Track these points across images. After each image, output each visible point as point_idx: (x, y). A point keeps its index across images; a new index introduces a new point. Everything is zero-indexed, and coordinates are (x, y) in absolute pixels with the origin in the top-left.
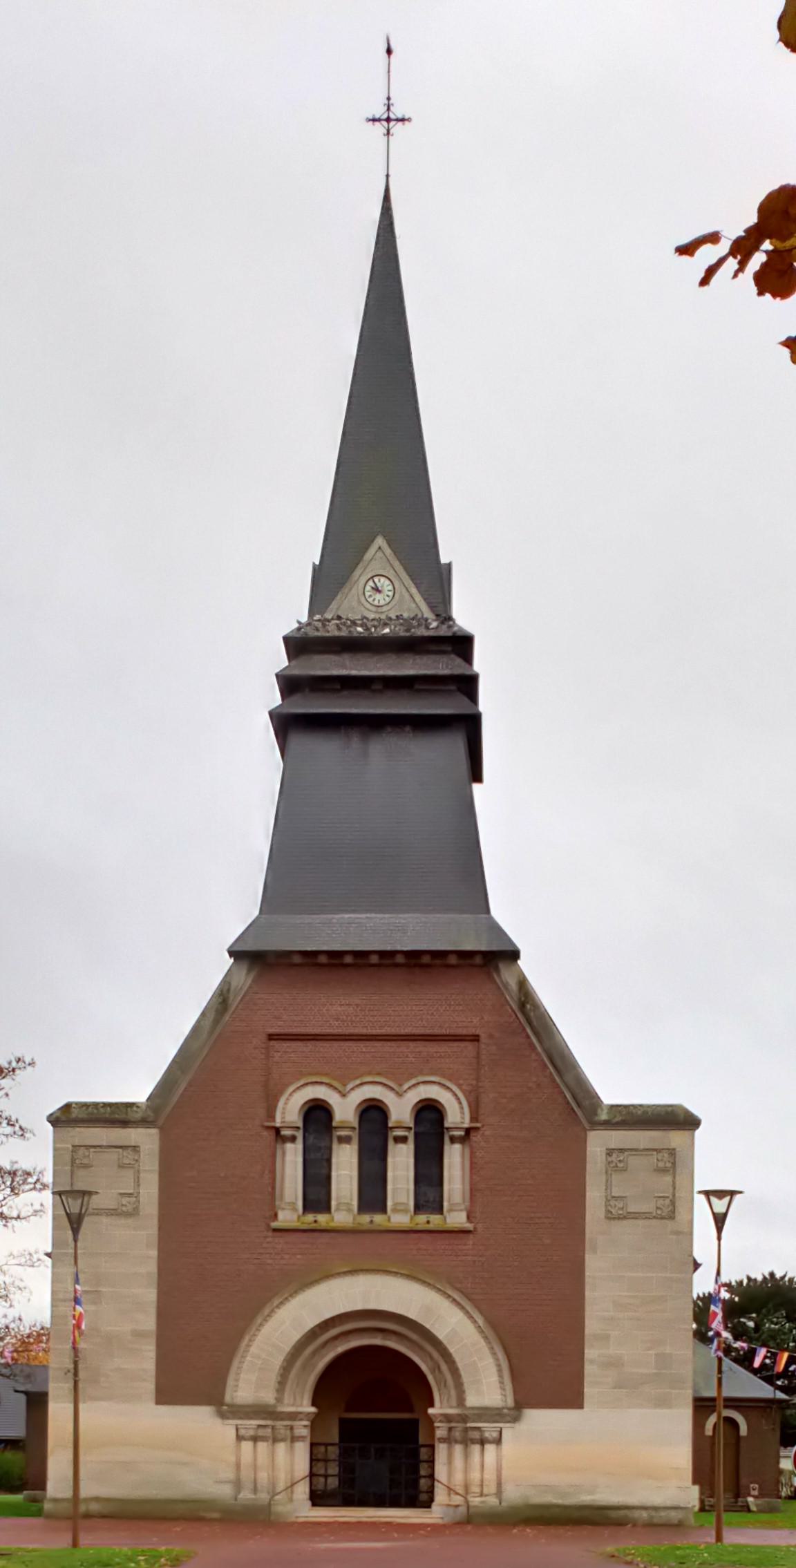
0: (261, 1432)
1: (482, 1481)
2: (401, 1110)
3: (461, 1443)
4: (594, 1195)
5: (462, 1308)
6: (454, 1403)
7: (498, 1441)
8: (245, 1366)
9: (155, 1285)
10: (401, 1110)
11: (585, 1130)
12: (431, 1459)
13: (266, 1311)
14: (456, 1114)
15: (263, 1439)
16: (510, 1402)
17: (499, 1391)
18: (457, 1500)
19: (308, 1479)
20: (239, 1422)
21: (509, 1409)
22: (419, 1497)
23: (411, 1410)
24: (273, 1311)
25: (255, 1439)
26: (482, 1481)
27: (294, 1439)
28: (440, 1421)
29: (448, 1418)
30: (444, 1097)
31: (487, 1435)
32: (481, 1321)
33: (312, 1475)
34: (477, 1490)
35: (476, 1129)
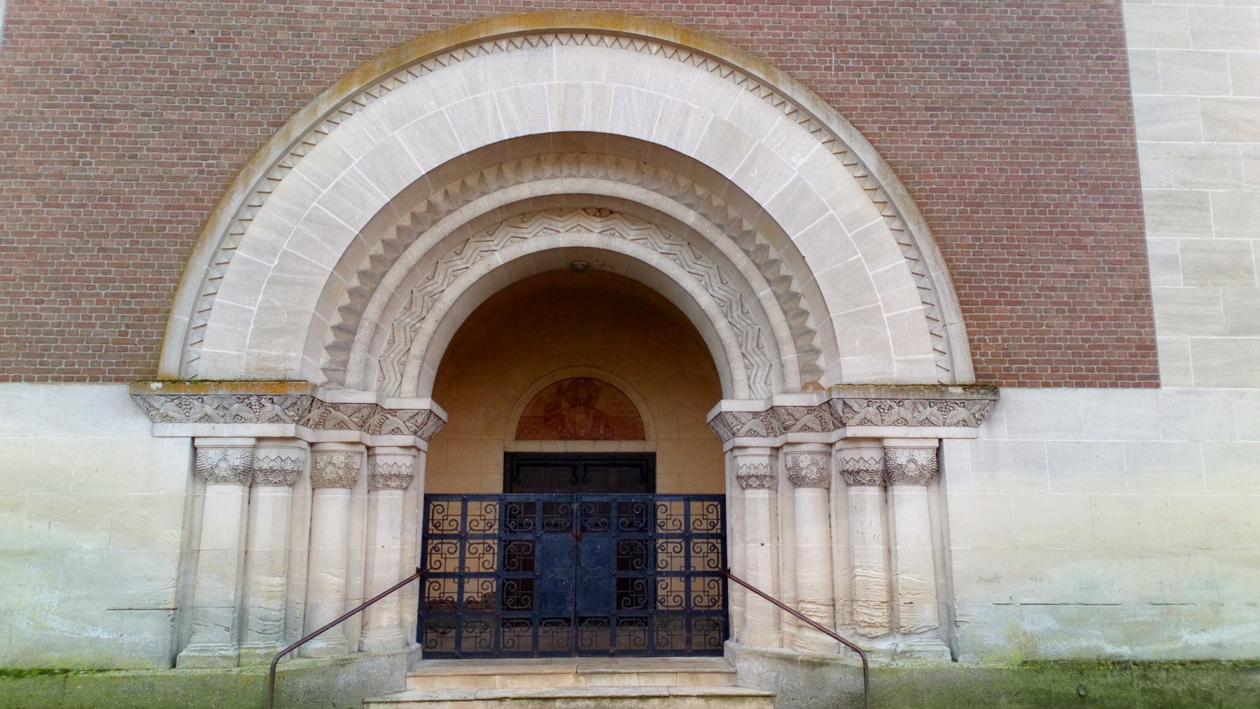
0: (268, 457)
1: (891, 589)
3: (814, 484)
5: (820, 128)
6: (794, 381)
7: (936, 473)
8: (230, 273)
12: (717, 530)
13: (298, 126)
15: (286, 478)
16: (965, 373)
17: (928, 342)
18: (814, 644)
19: (417, 582)
20: (202, 429)
21: (965, 387)
23: (638, 434)
24: (314, 129)
25: (249, 476)
26: (891, 589)
27: (377, 481)
28: (752, 433)
29: (775, 420)
31: (901, 458)
32: (870, 159)
33: (424, 574)
34: (880, 616)
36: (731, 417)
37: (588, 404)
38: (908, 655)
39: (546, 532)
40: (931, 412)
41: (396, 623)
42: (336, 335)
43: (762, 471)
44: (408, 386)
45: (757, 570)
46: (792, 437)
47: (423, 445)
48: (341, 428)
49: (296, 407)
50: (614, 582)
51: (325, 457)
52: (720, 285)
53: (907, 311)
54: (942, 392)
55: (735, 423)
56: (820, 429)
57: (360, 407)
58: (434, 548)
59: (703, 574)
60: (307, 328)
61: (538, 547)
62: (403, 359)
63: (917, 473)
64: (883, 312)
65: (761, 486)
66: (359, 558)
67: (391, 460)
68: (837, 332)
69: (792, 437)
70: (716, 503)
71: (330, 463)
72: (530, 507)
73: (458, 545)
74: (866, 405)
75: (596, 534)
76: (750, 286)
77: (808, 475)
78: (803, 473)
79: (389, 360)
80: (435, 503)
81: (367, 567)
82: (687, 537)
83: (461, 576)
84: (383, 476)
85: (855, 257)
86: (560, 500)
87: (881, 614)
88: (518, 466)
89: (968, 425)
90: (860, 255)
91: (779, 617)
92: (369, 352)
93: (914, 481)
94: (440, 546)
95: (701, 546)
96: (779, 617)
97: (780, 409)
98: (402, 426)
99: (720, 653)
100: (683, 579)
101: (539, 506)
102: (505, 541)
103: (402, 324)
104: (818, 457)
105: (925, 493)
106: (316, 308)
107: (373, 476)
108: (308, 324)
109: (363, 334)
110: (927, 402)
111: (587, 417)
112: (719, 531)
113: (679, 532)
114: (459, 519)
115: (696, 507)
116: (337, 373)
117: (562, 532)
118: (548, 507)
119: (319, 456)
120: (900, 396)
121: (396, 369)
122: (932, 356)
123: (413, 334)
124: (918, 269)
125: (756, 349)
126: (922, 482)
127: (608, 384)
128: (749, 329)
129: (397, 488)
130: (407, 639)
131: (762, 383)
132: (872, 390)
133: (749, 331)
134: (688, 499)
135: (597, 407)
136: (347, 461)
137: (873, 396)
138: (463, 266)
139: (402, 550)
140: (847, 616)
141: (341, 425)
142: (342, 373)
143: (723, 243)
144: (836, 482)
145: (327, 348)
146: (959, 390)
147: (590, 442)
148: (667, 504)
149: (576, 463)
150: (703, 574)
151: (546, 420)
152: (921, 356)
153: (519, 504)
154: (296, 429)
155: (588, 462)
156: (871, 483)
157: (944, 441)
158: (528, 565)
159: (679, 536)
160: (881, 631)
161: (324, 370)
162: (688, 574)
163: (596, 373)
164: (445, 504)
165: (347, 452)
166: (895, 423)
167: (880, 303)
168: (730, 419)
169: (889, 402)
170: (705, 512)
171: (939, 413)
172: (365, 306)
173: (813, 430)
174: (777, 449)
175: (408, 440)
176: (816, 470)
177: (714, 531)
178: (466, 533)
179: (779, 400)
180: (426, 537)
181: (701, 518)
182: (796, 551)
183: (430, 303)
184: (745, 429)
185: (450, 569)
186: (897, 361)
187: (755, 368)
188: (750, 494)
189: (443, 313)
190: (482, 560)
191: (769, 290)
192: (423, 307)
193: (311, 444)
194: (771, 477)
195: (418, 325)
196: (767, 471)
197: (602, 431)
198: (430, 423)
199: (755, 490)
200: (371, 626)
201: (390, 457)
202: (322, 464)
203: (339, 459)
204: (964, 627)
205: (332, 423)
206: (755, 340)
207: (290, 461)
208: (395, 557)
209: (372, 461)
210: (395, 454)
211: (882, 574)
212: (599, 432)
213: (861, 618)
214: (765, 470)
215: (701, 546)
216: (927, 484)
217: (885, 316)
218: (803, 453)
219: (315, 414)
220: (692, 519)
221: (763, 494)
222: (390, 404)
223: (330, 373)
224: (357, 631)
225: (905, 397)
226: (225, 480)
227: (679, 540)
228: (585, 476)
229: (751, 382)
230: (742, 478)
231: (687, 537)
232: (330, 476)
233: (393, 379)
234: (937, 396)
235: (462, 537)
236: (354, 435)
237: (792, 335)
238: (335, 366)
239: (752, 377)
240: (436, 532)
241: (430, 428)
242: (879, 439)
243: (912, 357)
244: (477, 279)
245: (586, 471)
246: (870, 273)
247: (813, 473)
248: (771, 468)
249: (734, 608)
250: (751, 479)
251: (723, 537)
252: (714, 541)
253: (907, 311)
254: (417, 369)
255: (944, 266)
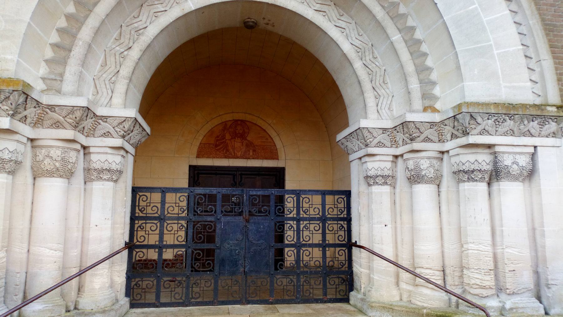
3: (430, 181)
6: (418, 104)
12: (344, 215)
17: (526, 74)
23: (274, 156)
28: (380, 145)
31: (507, 161)
33: (130, 246)
34: (489, 281)
36: (367, 131)
37: (243, 136)
38: (514, 310)
39: (224, 215)
41: (107, 285)
42: (53, 51)
43: (386, 173)
44: (118, 99)
45: (382, 244)
46: (416, 146)
47: (132, 150)
48: (58, 127)
49: (9, 102)
50: (273, 250)
51: (43, 151)
52: (357, 36)
53: (511, 49)
54: (542, 110)
55: (369, 137)
56: (437, 139)
57: (73, 109)
58: (140, 226)
59: (335, 246)
60: (22, 35)
61: (218, 226)
62: (113, 79)
63: (518, 172)
64: (494, 49)
65: (385, 183)
66: (76, 235)
67: (103, 158)
68: (461, 62)
69: (416, 146)
70: (343, 197)
71: (48, 156)
72: (212, 198)
73: (158, 224)
74: (486, 118)
75: (261, 218)
76: (385, 32)
77: (427, 175)
78: (423, 173)
79: (102, 79)
80: (141, 194)
81: (84, 241)
82: (323, 219)
83: (160, 247)
84: (96, 170)
85: (474, 6)
86: (234, 193)
87: (490, 279)
88: (198, 174)
89: (555, 137)
90: (477, 5)
91: (397, 277)
92: (83, 66)
93: (515, 178)
94: (144, 225)
95: (332, 226)
96: (397, 277)
97: (410, 123)
98: (112, 131)
99: (346, 300)
100: (321, 249)
101: (219, 197)
102: (194, 222)
103: (113, 51)
104: (435, 162)
105: (522, 188)
106: (31, 18)
107: (87, 170)
108: (23, 32)
109: (78, 51)
110: (531, 117)
111: (242, 145)
112: (345, 216)
113: (318, 216)
114: (159, 206)
115: (329, 199)
116: (54, 82)
117: (235, 215)
118: (226, 198)
119: (38, 151)
120: (512, 112)
121: (108, 86)
122: (529, 84)
123: (122, 59)
124: (518, 19)
125: (382, 84)
126: (521, 179)
127: (256, 124)
128: (377, 69)
129: (108, 180)
130: (116, 296)
131: (387, 109)
132: (492, 107)
133: (378, 71)
134: (324, 193)
135: (249, 138)
136: (63, 155)
137: (493, 111)
138: (163, 9)
139: (113, 228)
140: (456, 279)
141: (57, 125)
142: (59, 82)
144: (447, 181)
145: (46, 61)
146: (554, 109)
147: (245, 160)
148: (310, 197)
149: (235, 173)
150: (335, 246)
151: (216, 146)
152: (522, 84)
153: (205, 195)
154: (11, 122)
155: (243, 173)
156: (482, 180)
157: (538, 148)
158: (211, 239)
159: (318, 219)
160: (490, 292)
161: (43, 79)
162: (324, 246)
163: (248, 118)
164: (148, 194)
165: (63, 148)
166: (505, 134)
167: (492, 42)
168: (366, 133)
169: (504, 116)
170: (336, 203)
171: (538, 126)
172: (80, 29)
173: (432, 141)
174: (396, 157)
175: (118, 142)
176: (433, 171)
177: (342, 216)
178: (165, 216)
179: (410, 117)
180: (133, 218)
181: (333, 206)
182: (413, 230)
183: (136, 36)
184: (376, 141)
185: (152, 242)
186: (505, 87)
187: (382, 98)
188: (376, 189)
189: (147, 44)
190: (176, 236)
191: (400, 35)
192: (130, 39)
193: (32, 140)
194: (392, 177)
195: (126, 53)
196: (390, 173)
197: (251, 154)
198: (135, 132)
199: (380, 186)
200: (86, 289)
201: (102, 155)
202: (41, 157)
203: (56, 153)
204: (554, 288)
205: (49, 122)
206: (382, 78)
207: (7, 152)
208: (107, 233)
209: (87, 157)
210: (107, 153)
211: (490, 248)
212: (249, 154)
213: (473, 282)
214: (389, 172)
215: (332, 226)
216: (523, 181)
217: (495, 52)
218: (422, 158)
219: (31, 112)
220: (327, 207)
221: (386, 189)
222: (101, 111)
223: (48, 82)
224: (73, 294)
225: (516, 113)
227: (318, 222)
228: (241, 181)
229: (379, 107)
230: (371, 177)
231: (323, 219)
232: (48, 167)
233: (105, 94)
234: (539, 113)
235: (161, 219)
236: (69, 134)
237: (416, 70)
238: (53, 77)
239: (380, 104)
240: (141, 215)
241: (136, 136)
242: (489, 146)
243: (515, 84)
244: (174, 19)
245: (241, 178)
246: (484, 20)
247: (430, 173)
248: (392, 170)
249: (357, 268)
250: (379, 178)
251: (349, 220)
252: (342, 222)
253: (511, 49)
254: (125, 87)
255: (538, 16)
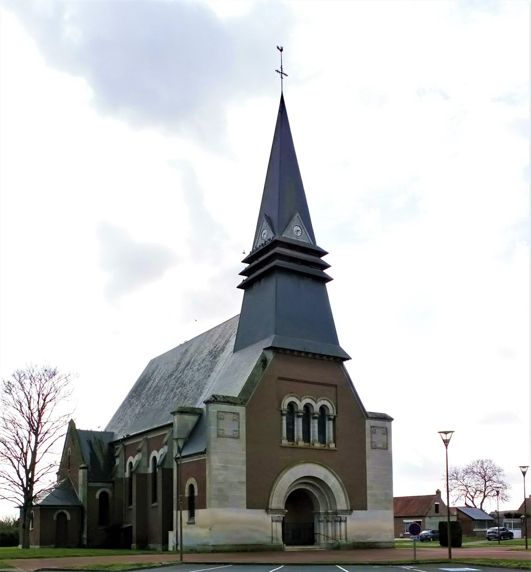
2: (316, 408)
4: (368, 440)
7: (345, 521)
9: (245, 465)
10: (316, 408)
11: (365, 419)
14: (331, 411)
16: (349, 509)
20: (273, 515)
21: (349, 510)
22: (311, 541)
30: (329, 405)
31: (342, 519)
32: (341, 481)
35: (337, 416)
40: (346, 513)
143: (322, 489)
221: (322, 523)
226: (274, 522)
242: (340, 517)
